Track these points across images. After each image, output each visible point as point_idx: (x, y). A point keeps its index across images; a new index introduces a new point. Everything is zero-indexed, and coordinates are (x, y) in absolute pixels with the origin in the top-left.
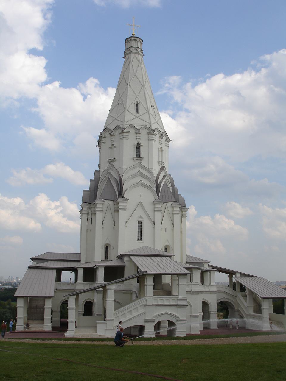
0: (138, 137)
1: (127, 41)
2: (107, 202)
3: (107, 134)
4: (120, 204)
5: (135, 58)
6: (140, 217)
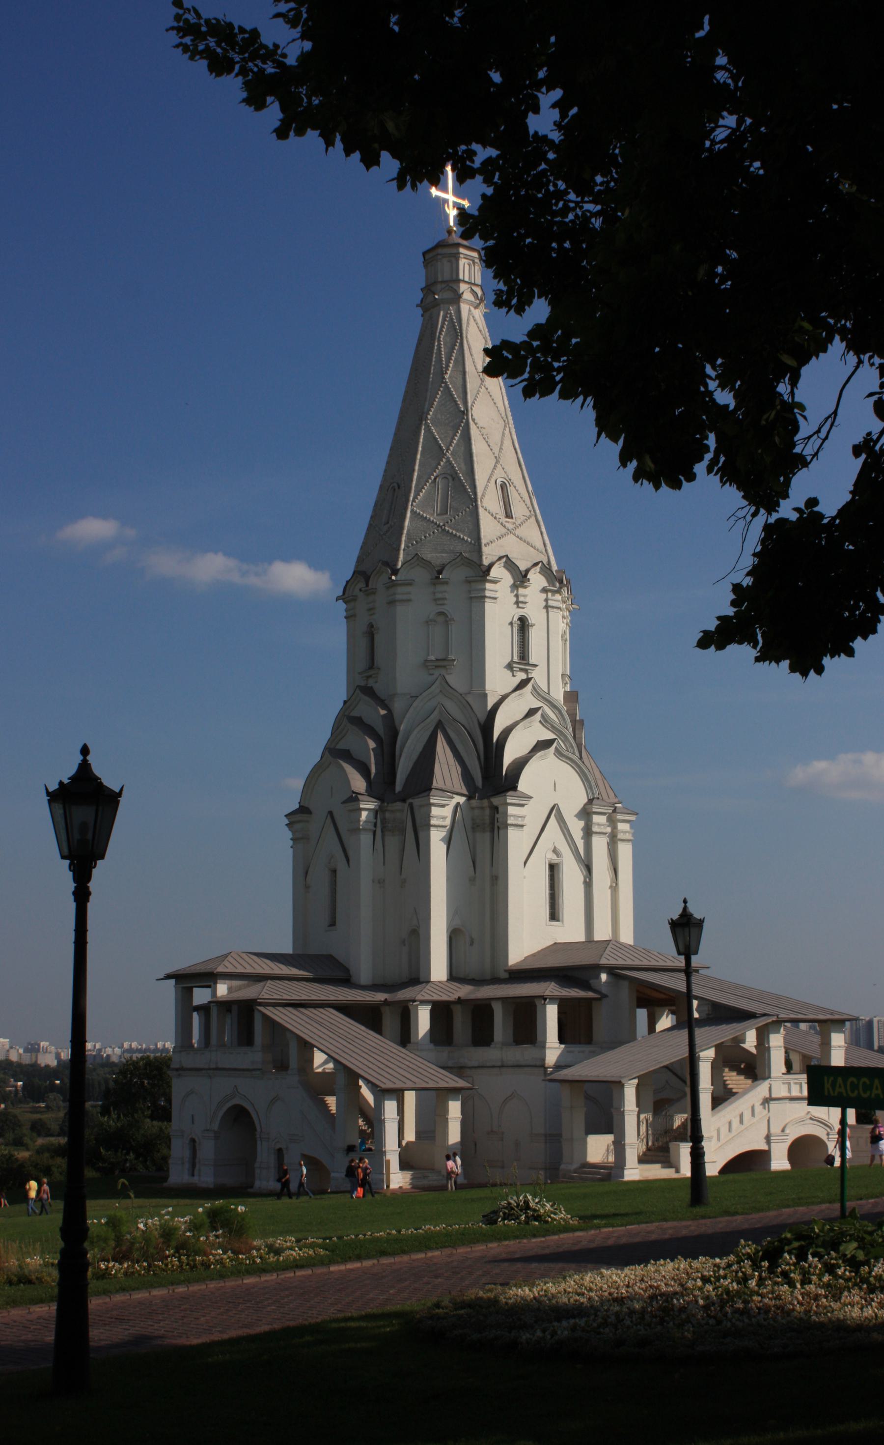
0: (521, 599)
3: (421, 575)
4: (511, 810)
5: (472, 319)
6: (555, 851)
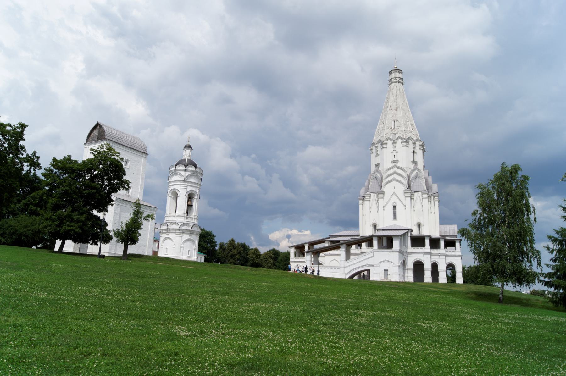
1: (390, 73)
2: (372, 195)
